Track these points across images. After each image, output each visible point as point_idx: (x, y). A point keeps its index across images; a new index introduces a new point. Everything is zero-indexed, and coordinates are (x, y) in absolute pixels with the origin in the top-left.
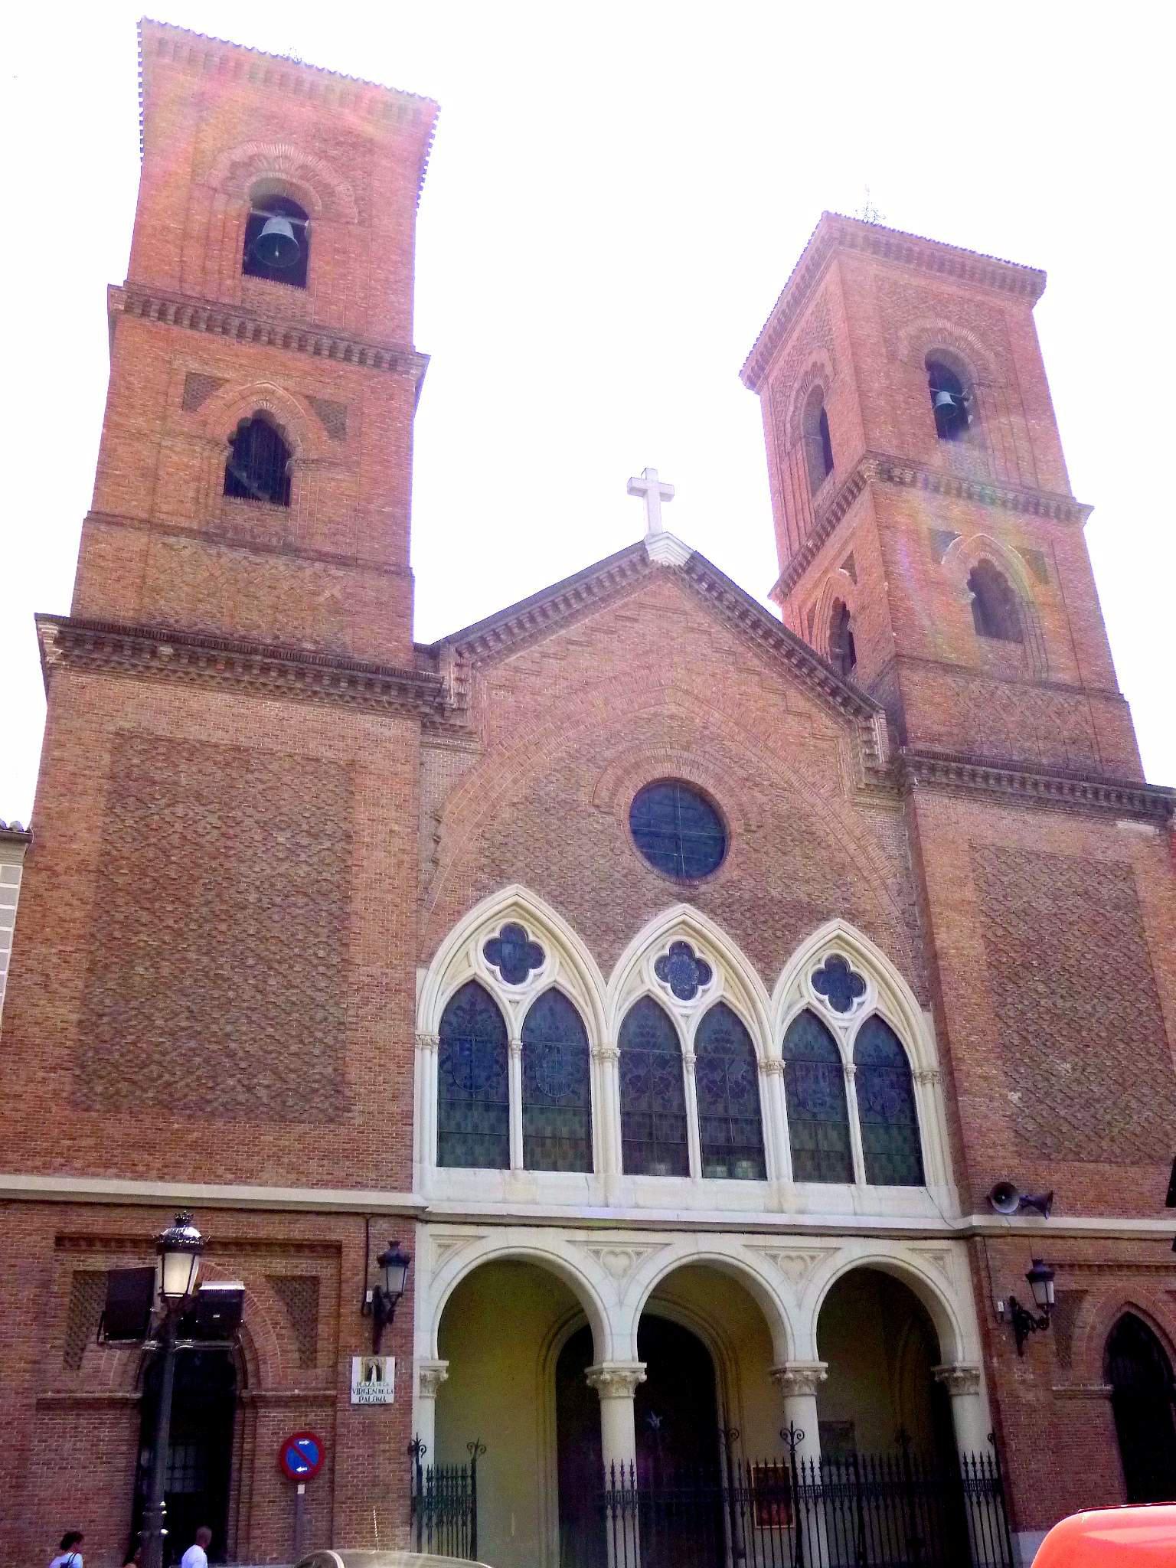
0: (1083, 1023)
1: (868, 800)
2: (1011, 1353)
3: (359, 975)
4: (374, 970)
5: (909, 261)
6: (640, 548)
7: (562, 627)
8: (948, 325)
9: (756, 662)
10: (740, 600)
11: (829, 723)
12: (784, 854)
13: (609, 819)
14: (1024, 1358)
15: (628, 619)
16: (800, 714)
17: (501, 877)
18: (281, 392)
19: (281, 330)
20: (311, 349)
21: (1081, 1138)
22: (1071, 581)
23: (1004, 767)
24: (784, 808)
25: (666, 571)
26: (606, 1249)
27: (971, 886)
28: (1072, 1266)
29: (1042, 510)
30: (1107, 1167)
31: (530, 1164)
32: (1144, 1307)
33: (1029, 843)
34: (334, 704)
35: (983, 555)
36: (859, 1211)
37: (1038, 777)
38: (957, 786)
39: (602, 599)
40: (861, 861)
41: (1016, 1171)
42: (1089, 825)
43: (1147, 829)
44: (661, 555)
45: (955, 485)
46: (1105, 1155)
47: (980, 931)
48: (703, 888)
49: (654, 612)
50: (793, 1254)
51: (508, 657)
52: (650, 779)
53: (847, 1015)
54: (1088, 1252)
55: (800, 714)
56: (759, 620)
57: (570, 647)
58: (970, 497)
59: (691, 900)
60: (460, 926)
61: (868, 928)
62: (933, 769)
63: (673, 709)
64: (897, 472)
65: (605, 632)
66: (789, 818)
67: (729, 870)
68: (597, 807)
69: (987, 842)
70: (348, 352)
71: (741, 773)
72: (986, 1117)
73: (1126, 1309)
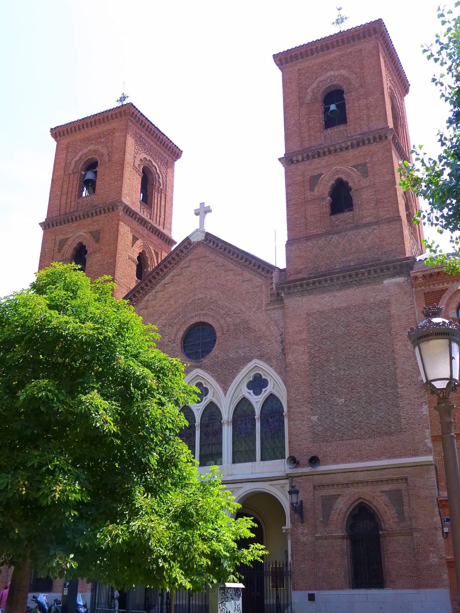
0: (352, 379)
1: (273, 307)
2: (299, 522)
5: (312, 54)
6: (187, 239)
7: (162, 280)
8: (332, 73)
9: (232, 265)
10: (223, 244)
11: (259, 280)
12: (237, 339)
13: (174, 345)
15: (186, 267)
16: (248, 280)
18: (83, 234)
19: (81, 214)
20: (90, 216)
21: (345, 430)
22: (380, 170)
23: (348, 271)
24: (238, 321)
25: (199, 244)
27: (305, 332)
28: (333, 485)
29: (366, 142)
30: (355, 441)
31: (263, 459)
32: (368, 499)
33: (336, 305)
35: (337, 177)
36: (253, 472)
37: (338, 275)
38: (302, 291)
39: (175, 264)
40: (268, 333)
42: (369, 287)
43: (400, 280)
44: (194, 240)
45: (321, 151)
46: (356, 436)
47: (307, 351)
48: (205, 361)
49: (196, 261)
51: (144, 297)
52: (189, 325)
53: (259, 396)
54: (340, 478)
55: (248, 280)
56: (230, 250)
57: (166, 286)
58: (330, 152)
59: (198, 367)
61: (268, 361)
62: (289, 288)
63: (200, 296)
64: (294, 159)
65: (178, 275)
66: (240, 324)
67: (215, 351)
68: (170, 341)
69: (315, 311)
70: (100, 211)
71: (223, 312)
72: (300, 429)
73: (360, 501)
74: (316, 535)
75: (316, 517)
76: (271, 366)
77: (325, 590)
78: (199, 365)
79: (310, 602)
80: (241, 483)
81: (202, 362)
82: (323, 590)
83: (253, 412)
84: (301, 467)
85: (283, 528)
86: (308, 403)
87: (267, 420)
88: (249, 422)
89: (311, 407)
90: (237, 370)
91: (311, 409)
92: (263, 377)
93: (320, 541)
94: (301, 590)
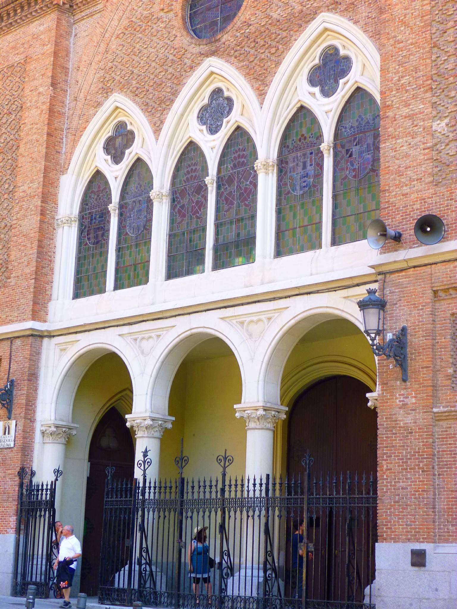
2: (396, 379)
3: (19, 194)
4: (25, 187)
13: (171, 15)
14: (408, 383)
17: (107, 92)
26: (140, 336)
34: (20, 25)
41: (430, 201)
50: (255, 319)
59: (213, 53)
60: (83, 139)
72: (407, 156)
74: (435, 410)
75: (438, 367)
76: (356, 23)
77: (452, 542)
78: (214, 48)
79: (416, 568)
80: (286, 297)
81: (219, 40)
82: (447, 541)
83: (319, 137)
84: (405, 249)
85: (368, 395)
86: (426, 92)
87: (347, 151)
88: (311, 161)
89: (435, 99)
90: (287, 44)
91: (434, 105)
92: (342, 52)
93: (444, 424)
94: (396, 540)
